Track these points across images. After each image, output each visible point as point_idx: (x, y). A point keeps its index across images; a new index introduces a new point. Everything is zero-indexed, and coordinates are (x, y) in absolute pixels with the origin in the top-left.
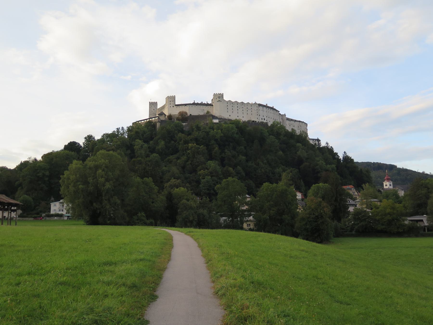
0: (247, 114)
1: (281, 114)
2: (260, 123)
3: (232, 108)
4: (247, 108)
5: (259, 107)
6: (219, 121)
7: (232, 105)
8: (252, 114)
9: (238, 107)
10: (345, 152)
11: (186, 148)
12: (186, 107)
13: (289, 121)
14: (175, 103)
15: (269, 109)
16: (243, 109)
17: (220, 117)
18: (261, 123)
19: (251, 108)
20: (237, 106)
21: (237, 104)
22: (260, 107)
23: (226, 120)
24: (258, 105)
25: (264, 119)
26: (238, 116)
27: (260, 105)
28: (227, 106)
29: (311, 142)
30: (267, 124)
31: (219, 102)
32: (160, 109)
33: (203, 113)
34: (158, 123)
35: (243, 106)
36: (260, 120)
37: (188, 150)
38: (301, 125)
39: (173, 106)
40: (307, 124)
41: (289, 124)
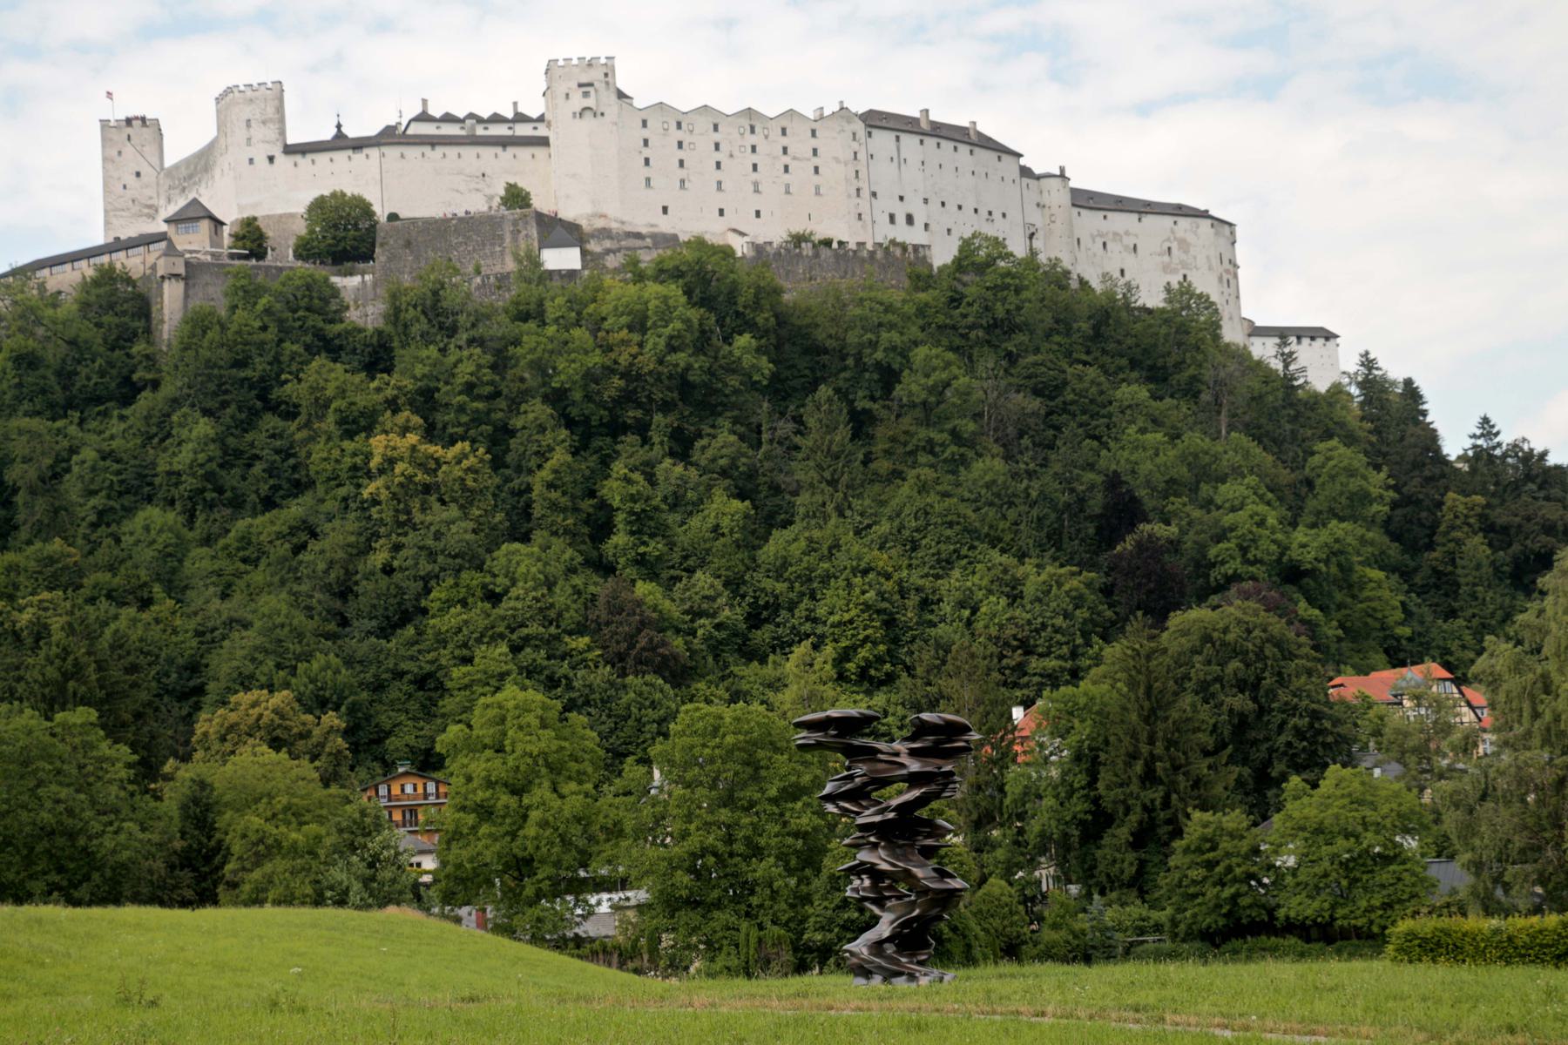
0: (788, 192)
1: (1037, 171)
2: (872, 254)
3: (681, 154)
4: (785, 150)
5: (870, 134)
6: (584, 253)
7: (680, 135)
8: (818, 193)
9: (717, 147)
10: (1486, 420)
11: (358, 460)
12: (359, 157)
13: (1102, 213)
14: (282, 133)
15: (944, 143)
16: (754, 158)
17: (599, 224)
18: (879, 255)
19: (815, 152)
20: (717, 137)
21: (716, 128)
22: (875, 132)
23: (638, 243)
24: (859, 127)
25: (910, 220)
26: (721, 212)
27: (875, 121)
28: (646, 142)
29: (1264, 350)
30: (925, 257)
31: (588, 121)
32: (184, 172)
33: (479, 195)
34: (166, 285)
35: (753, 139)
36: (884, 233)
37: (370, 476)
38: (1190, 238)
39: (271, 159)
40: (1230, 225)
41: (1101, 235)
